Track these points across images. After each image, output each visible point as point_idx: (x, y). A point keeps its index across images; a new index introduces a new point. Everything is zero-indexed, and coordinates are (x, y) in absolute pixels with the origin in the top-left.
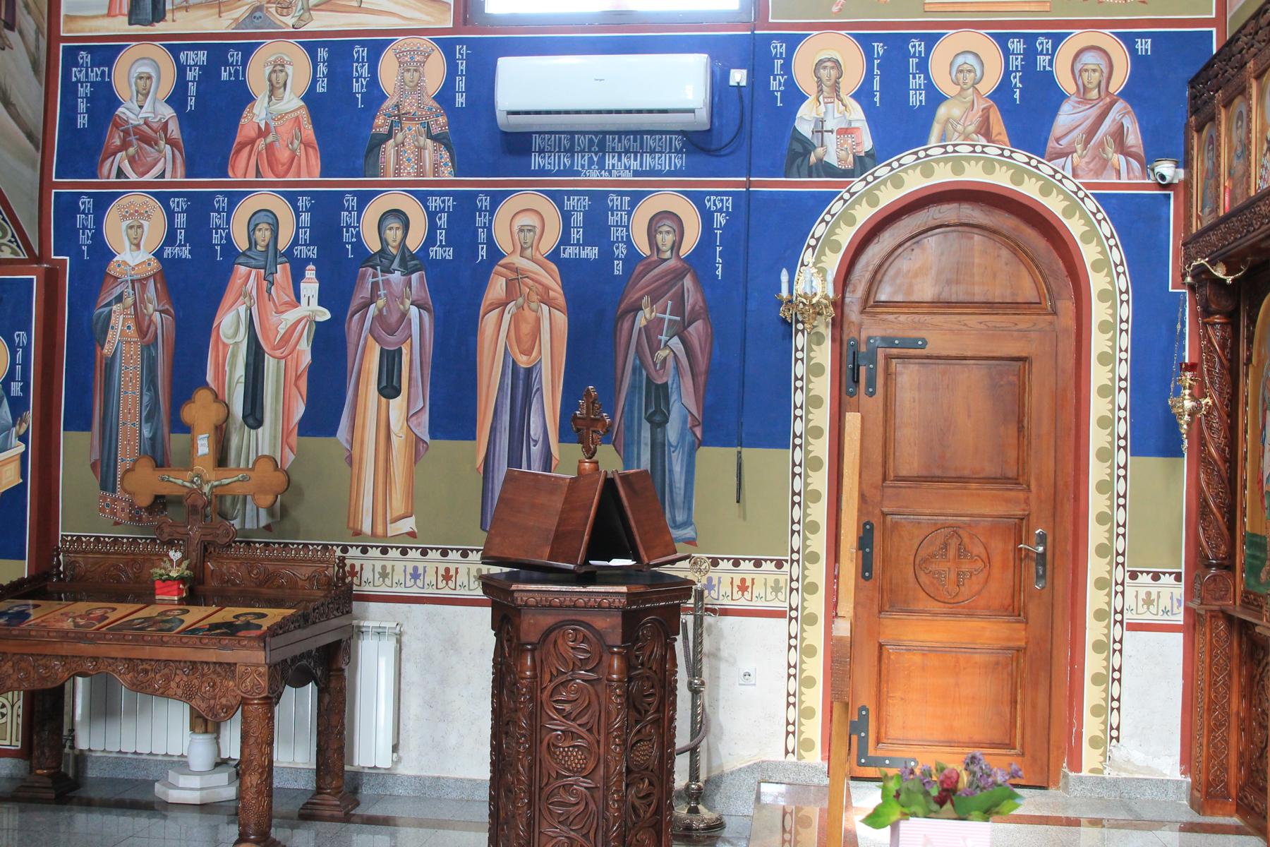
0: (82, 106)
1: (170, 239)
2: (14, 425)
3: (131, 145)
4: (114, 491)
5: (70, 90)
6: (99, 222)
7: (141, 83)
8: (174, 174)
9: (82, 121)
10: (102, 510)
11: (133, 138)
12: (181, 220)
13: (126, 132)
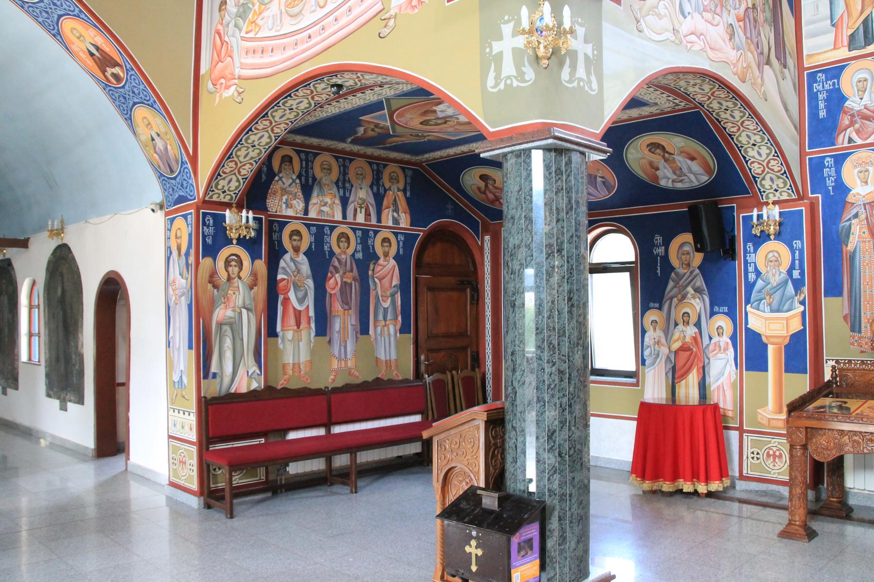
0: (822, 105)
2: (796, 295)
3: (855, 122)
4: (860, 332)
5: (813, 97)
6: (838, 172)
7: (860, 84)
9: (822, 114)
10: (852, 344)
11: (857, 118)
13: (853, 116)
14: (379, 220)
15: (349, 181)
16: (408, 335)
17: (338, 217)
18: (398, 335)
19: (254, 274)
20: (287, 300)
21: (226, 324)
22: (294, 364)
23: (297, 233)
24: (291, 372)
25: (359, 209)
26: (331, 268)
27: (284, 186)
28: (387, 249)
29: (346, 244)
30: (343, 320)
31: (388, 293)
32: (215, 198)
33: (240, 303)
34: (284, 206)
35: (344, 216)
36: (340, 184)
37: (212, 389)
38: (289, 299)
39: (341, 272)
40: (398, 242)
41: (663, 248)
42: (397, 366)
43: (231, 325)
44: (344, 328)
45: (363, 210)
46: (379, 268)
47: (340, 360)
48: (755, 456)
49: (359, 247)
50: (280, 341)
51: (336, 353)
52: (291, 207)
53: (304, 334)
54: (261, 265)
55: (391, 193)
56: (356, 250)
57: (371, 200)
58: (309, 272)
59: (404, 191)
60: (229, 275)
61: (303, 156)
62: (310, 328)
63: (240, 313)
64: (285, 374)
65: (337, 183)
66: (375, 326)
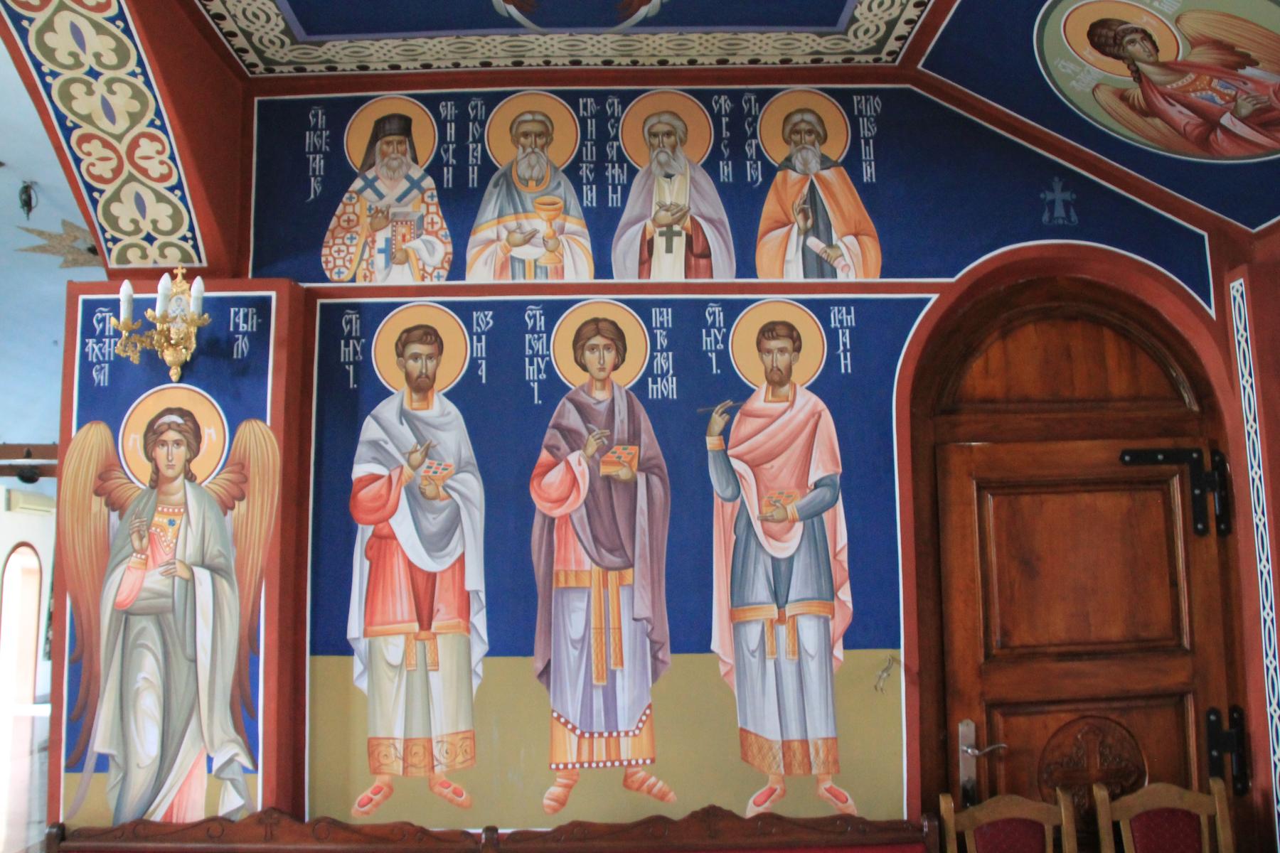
14: (746, 265)
15: (621, 159)
16: (883, 654)
17: (579, 269)
18: (839, 651)
19: (238, 467)
20: (384, 541)
21: (144, 613)
22: (408, 742)
23: (429, 334)
24: (398, 767)
25: (660, 243)
26: (551, 436)
27: (381, 204)
28: (782, 361)
29: (610, 357)
30: (601, 606)
31: (792, 509)
33: (190, 551)
34: (380, 260)
35: (603, 266)
36: (585, 171)
37: (92, 803)
38: (393, 537)
39: (592, 446)
40: (832, 336)
42: (834, 764)
43: (158, 615)
44: (603, 630)
45: (680, 243)
46: (751, 425)
47: (586, 734)
49: (664, 362)
50: (357, 665)
51: (573, 711)
52: (406, 259)
53: (446, 647)
54: (262, 440)
55: (793, 176)
56: (649, 371)
57: (712, 206)
58: (468, 452)
59: (852, 164)
60: (157, 470)
61: (448, 110)
62: (469, 628)
63: (191, 582)
64: (376, 771)
65: (572, 172)
66: (737, 623)
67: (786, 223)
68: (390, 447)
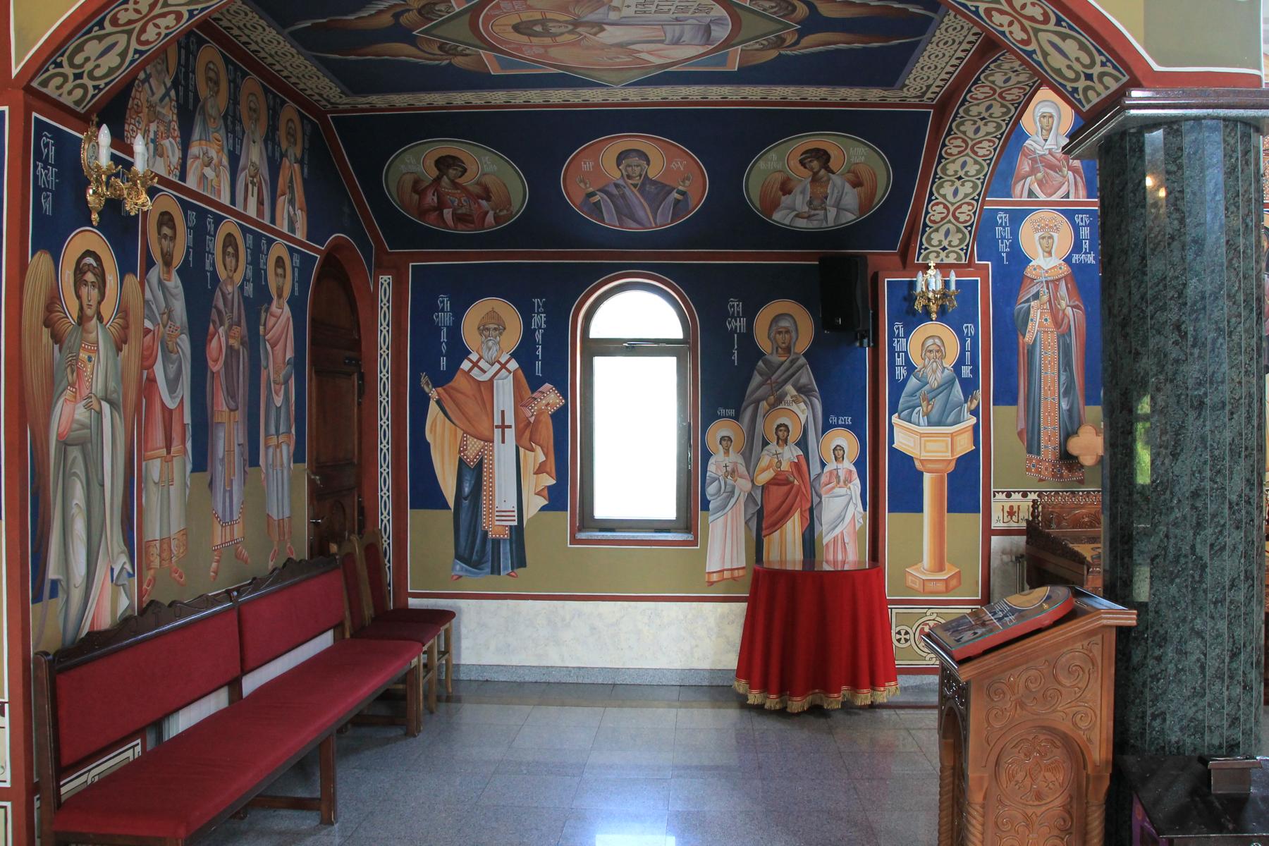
1: (1077, 248)
2: (966, 401)
4: (1039, 454)
6: (1015, 233)
7: (1045, 120)
8: (1077, 195)
10: (1029, 470)
12: (1085, 232)
13: (1034, 160)
32: (50, 91)
33: (98, 388)
41: (744, 320)
48: (903, 637)
49: (250, 274)
56: (245, 279)
59: (301, 162)
63: (100, 413)
67: (284, 194)
68: (154, 307)
